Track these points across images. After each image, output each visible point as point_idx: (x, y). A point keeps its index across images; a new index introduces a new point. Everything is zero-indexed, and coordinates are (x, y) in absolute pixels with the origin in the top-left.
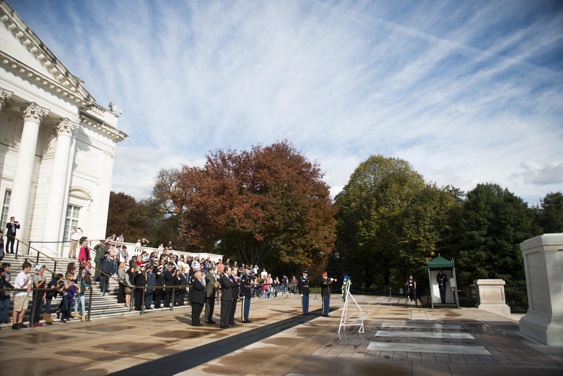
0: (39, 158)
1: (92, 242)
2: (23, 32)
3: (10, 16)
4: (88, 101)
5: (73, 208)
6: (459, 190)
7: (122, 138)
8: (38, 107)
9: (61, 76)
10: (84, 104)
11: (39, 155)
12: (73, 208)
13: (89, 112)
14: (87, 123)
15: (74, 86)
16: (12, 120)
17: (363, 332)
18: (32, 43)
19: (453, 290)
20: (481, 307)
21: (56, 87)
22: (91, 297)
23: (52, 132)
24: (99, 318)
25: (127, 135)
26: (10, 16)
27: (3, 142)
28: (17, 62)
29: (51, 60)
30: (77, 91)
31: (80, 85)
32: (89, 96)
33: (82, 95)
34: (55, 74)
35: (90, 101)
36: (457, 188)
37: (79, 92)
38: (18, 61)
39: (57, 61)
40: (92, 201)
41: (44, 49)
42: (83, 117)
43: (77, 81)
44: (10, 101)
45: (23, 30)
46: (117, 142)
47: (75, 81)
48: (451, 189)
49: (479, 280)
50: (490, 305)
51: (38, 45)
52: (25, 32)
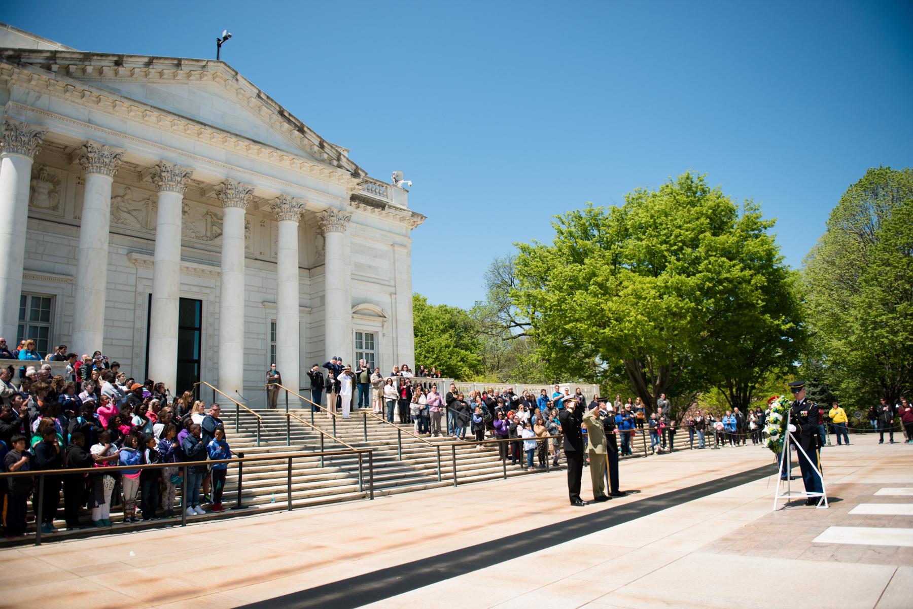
9: (316, 148)
11: (307, 267)
23: (318, 231)
27: (258, 258)
29: (297, 129)
30: (339, 166)
31: (342, 157)
39: (306, 129)
43: (337, 151)
47: (334, 151)
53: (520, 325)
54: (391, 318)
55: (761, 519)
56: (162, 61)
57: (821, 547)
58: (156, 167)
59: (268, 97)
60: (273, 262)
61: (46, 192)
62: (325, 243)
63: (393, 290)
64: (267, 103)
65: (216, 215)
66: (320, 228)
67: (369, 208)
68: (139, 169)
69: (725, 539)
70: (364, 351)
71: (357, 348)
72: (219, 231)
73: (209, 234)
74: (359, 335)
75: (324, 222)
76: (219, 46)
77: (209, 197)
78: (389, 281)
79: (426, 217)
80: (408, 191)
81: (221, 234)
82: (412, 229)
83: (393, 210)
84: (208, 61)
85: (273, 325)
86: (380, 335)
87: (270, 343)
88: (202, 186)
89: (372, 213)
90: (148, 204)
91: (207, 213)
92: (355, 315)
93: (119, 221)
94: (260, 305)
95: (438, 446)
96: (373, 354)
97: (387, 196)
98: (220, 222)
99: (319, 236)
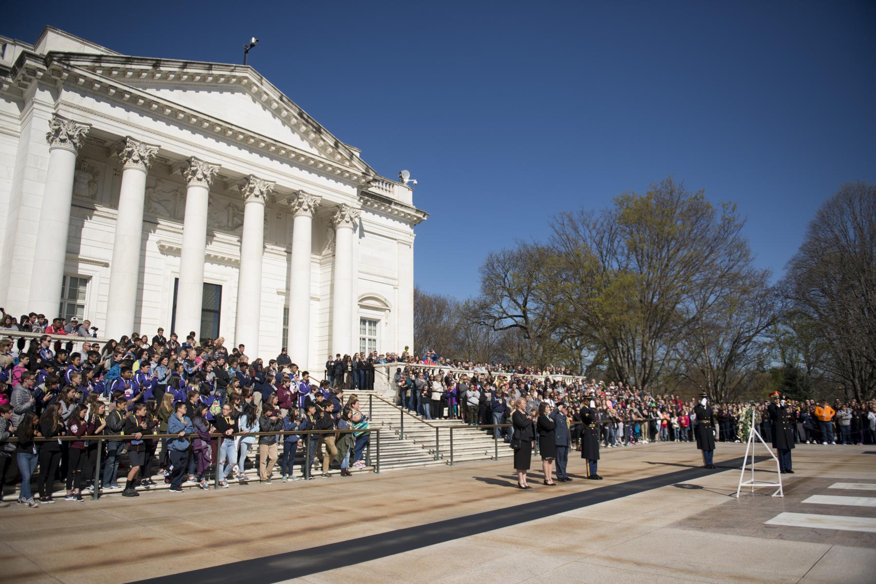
1: (390, 368)
2: (277, 102)
3: (259, 84)
4: (368, 175)
5: (367, 324)
7: (421, 218)
8: (307, 195)
9: (330, 150)
10: (364, 180)
12: (367, 324)
13: (374, 189)
14: (372, 205)
16: (281, 216)
17: (782, 495)
18: (290, 114)
21: (326, 166)
22: (378, 441)
23: (330, 224)
24: (393, 469)
26: (259, 84)
28: (274, 142)
29: (314, 130)
30: (352, 166)
31: (354, 157)
33: (358, 168)
34: (323, 149)
37: (355, 166)
38: (276, 141)
39: (322, 130)
40: (390, 311)
41: (304, 118)
42: (366, 198)
43: (350, 151)
44: (274, 194)
45: (277, 99)
46: (415, 225)
51: (296, 115)
52: (279, 101)
53: (511, 317)
55: (724, 504)
56: (195, 65)
57: (769, 527)
58: (187, 162)
61: (86, 181)
62: (335, 236)
63: (396, 282)
65: (237, 207)
68: (169, 163)
69: (691, 519)
70: (367, 336)
72: (239, 222)
73: (230, 224)
74: (363, 321)
76: (247, 52)
77: (232, 190)
81: (242, 225)
82: (415, 225)
84: (236, 66)
85: (286, 311)
88: (225, 180)
90: (176, 195)
91: (229, 205)
93: (151, 210)
94: (275, 291)
95: (437, 428)
97: (393, 192)
98: (241, 213)
99: (331, 229)
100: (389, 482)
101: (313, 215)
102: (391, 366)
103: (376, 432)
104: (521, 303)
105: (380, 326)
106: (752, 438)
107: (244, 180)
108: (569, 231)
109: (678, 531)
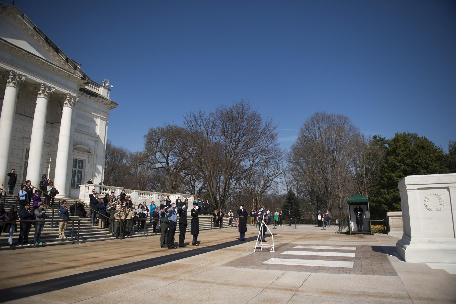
0: (50, 124)
1: (89, 187)
6: (385, 139)
15: (73, 69)
17: (274, 251)
19: (368, 220)
20: (390, 233)
25: (118, 104)
27: (22, 114)
31: (77, 68)
32: (84, 76)
33: (79, 75)
35: (86, 80)
36: (383, 138)
39: (59, 51)
43: (75, 65)
47: (74, 65)
48: (378, 139)
49: (389, 212)
50: (397, 232)
51: (43, 39)
52: (33, 30)
53: (160, 163)
54: (94, 154)
55: (248, 255)
59: (40, 31)
60: (31, 117)
63: (97, 140)
64: (39, 34)
66: (60, 103)
67: (88, 96)
69: (232, 262)
70: (77, 169)
71: (73, 167)
74: (75, 161)
75: (63, 100)
78: (94, 134)
79: (118, 105)
80: (110, 90)
82: (110, 110)
83: (101, 99)
84: (7, 5)
86: (87, 162)
87: (24, 160)
89: (90, 99)
92: (74, 150)
96: (81, 171)
98: (2, 92)
99: (59, 107)
100: (83, 249)
101: (49, 98)
102: (90, 186)
103: (78, 222)
104: (166, 156)
105: (85, 164)
106: (262, 226)
107: (7, 72)
108: (193, 121)
109: (225, 267)
